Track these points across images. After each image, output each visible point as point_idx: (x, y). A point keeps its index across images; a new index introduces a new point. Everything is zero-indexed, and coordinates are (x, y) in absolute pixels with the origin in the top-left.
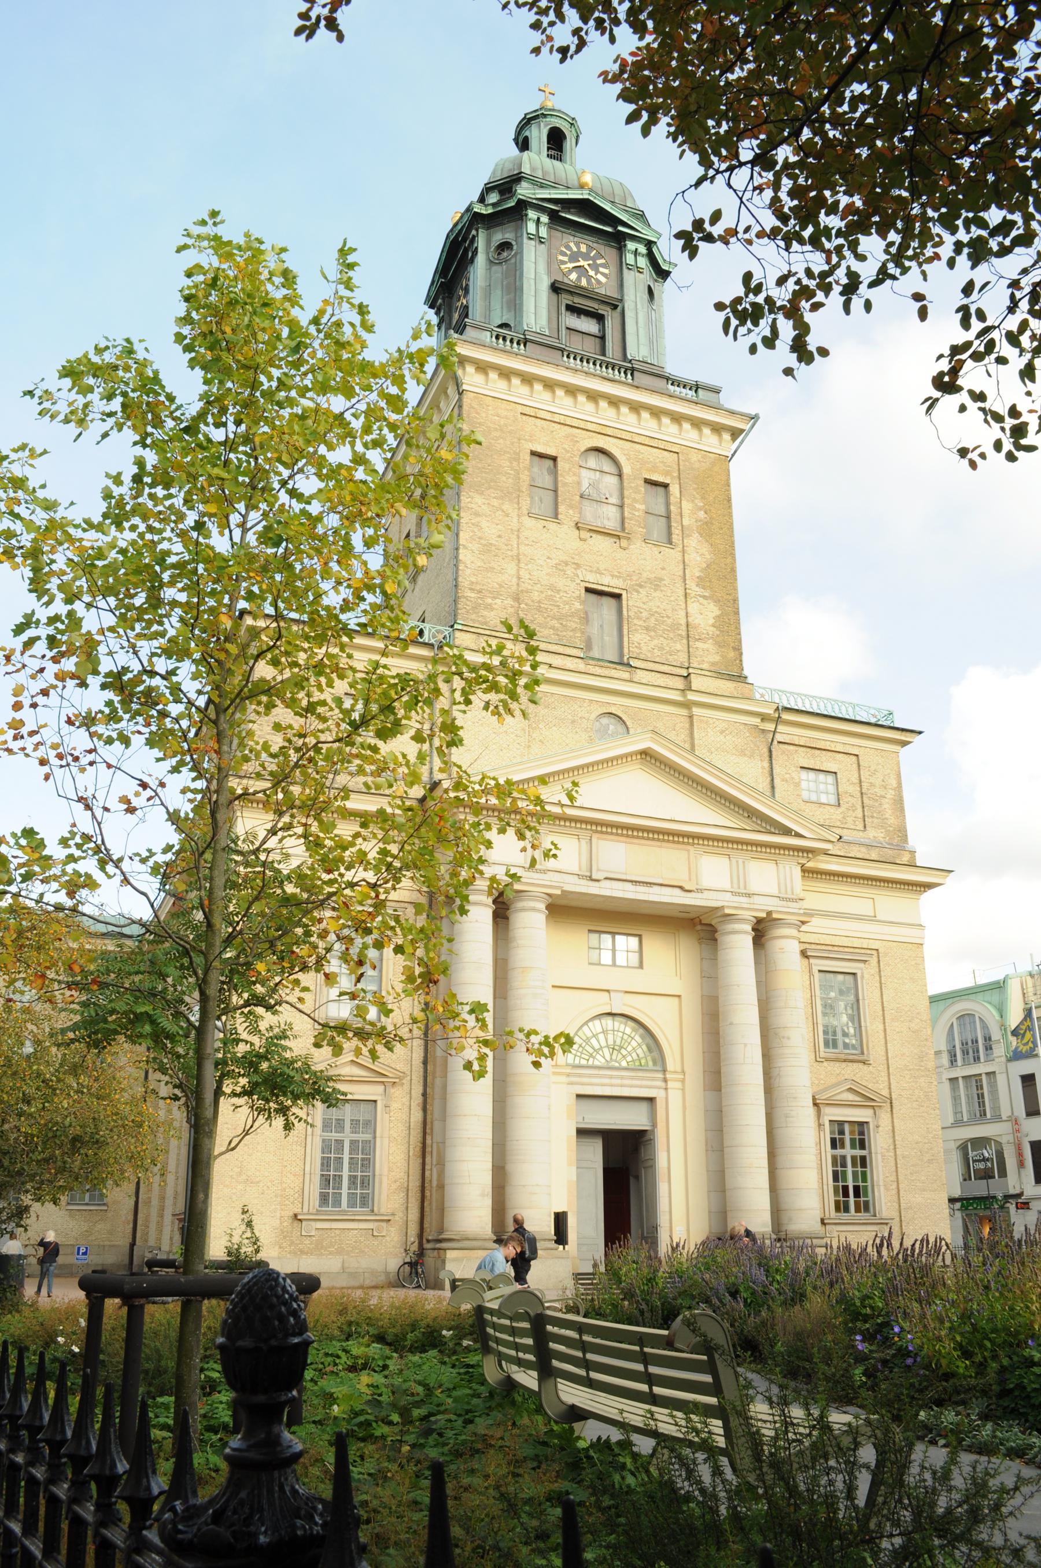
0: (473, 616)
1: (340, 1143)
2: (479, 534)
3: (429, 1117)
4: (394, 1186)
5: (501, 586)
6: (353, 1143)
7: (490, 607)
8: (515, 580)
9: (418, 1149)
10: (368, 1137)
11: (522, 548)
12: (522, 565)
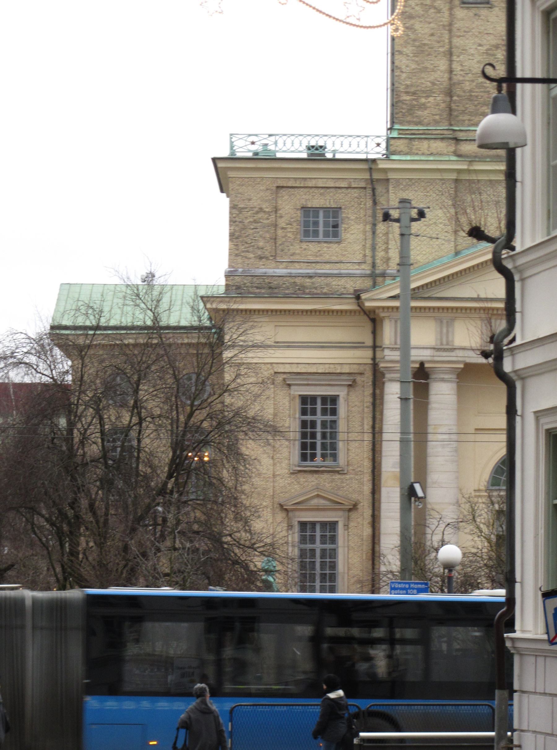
0: (409, 118)
1: (313, 551)
2: (412, 36)
3: (377, 532)
4: (352, 580)
5: (433, 84)
6: (323, 551)
7: (423, 107)
8: (446, 75)
9: (370, 554)
10: (332, 546)
11: (455, 41)
12: (455, 58)
